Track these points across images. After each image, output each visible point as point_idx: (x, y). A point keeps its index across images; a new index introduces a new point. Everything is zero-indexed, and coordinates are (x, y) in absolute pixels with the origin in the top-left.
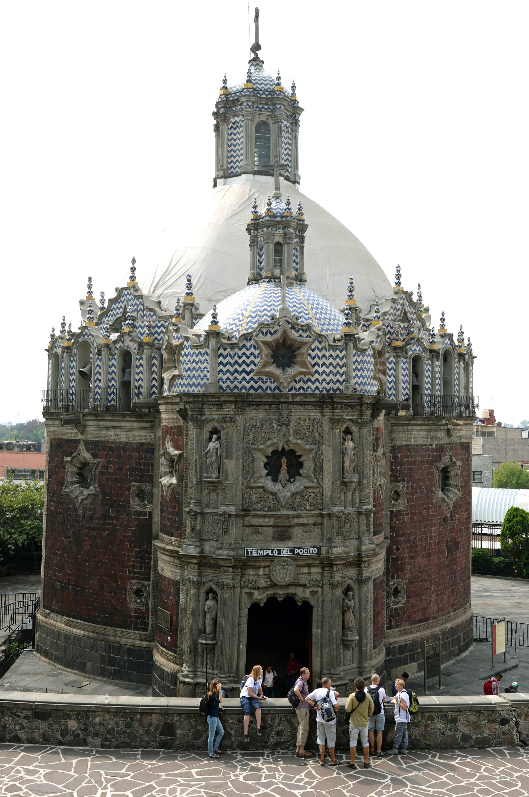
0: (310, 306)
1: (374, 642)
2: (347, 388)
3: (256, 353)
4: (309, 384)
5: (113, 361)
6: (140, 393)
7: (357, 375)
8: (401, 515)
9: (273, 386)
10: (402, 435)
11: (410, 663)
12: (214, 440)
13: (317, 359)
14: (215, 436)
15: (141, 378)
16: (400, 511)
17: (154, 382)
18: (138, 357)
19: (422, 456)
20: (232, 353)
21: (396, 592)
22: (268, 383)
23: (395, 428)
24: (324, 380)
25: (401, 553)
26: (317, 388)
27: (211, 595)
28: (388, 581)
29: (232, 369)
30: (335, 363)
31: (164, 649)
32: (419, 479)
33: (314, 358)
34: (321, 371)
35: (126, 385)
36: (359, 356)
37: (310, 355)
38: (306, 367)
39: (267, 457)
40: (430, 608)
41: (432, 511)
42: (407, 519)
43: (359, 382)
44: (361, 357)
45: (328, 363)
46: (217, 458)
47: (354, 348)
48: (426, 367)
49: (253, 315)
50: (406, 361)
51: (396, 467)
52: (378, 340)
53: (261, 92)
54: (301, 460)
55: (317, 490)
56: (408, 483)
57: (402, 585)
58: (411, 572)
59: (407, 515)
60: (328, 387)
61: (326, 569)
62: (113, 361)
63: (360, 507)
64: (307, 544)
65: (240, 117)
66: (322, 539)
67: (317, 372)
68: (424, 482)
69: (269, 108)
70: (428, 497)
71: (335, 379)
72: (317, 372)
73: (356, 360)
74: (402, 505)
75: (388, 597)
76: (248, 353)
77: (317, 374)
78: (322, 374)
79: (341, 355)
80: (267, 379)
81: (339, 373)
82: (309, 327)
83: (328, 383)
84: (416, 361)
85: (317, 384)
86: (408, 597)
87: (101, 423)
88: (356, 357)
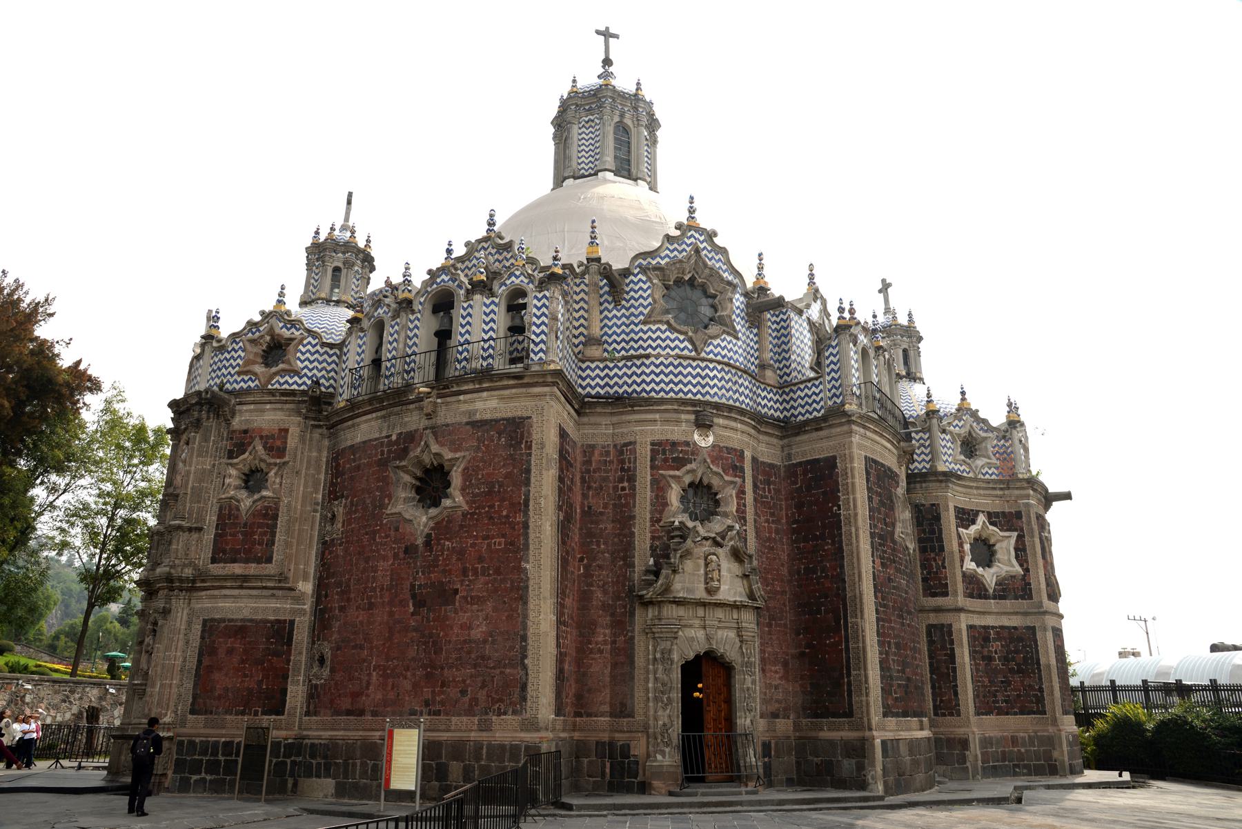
40: (368, 696)
42: (340, 551)
58: (339, 632)
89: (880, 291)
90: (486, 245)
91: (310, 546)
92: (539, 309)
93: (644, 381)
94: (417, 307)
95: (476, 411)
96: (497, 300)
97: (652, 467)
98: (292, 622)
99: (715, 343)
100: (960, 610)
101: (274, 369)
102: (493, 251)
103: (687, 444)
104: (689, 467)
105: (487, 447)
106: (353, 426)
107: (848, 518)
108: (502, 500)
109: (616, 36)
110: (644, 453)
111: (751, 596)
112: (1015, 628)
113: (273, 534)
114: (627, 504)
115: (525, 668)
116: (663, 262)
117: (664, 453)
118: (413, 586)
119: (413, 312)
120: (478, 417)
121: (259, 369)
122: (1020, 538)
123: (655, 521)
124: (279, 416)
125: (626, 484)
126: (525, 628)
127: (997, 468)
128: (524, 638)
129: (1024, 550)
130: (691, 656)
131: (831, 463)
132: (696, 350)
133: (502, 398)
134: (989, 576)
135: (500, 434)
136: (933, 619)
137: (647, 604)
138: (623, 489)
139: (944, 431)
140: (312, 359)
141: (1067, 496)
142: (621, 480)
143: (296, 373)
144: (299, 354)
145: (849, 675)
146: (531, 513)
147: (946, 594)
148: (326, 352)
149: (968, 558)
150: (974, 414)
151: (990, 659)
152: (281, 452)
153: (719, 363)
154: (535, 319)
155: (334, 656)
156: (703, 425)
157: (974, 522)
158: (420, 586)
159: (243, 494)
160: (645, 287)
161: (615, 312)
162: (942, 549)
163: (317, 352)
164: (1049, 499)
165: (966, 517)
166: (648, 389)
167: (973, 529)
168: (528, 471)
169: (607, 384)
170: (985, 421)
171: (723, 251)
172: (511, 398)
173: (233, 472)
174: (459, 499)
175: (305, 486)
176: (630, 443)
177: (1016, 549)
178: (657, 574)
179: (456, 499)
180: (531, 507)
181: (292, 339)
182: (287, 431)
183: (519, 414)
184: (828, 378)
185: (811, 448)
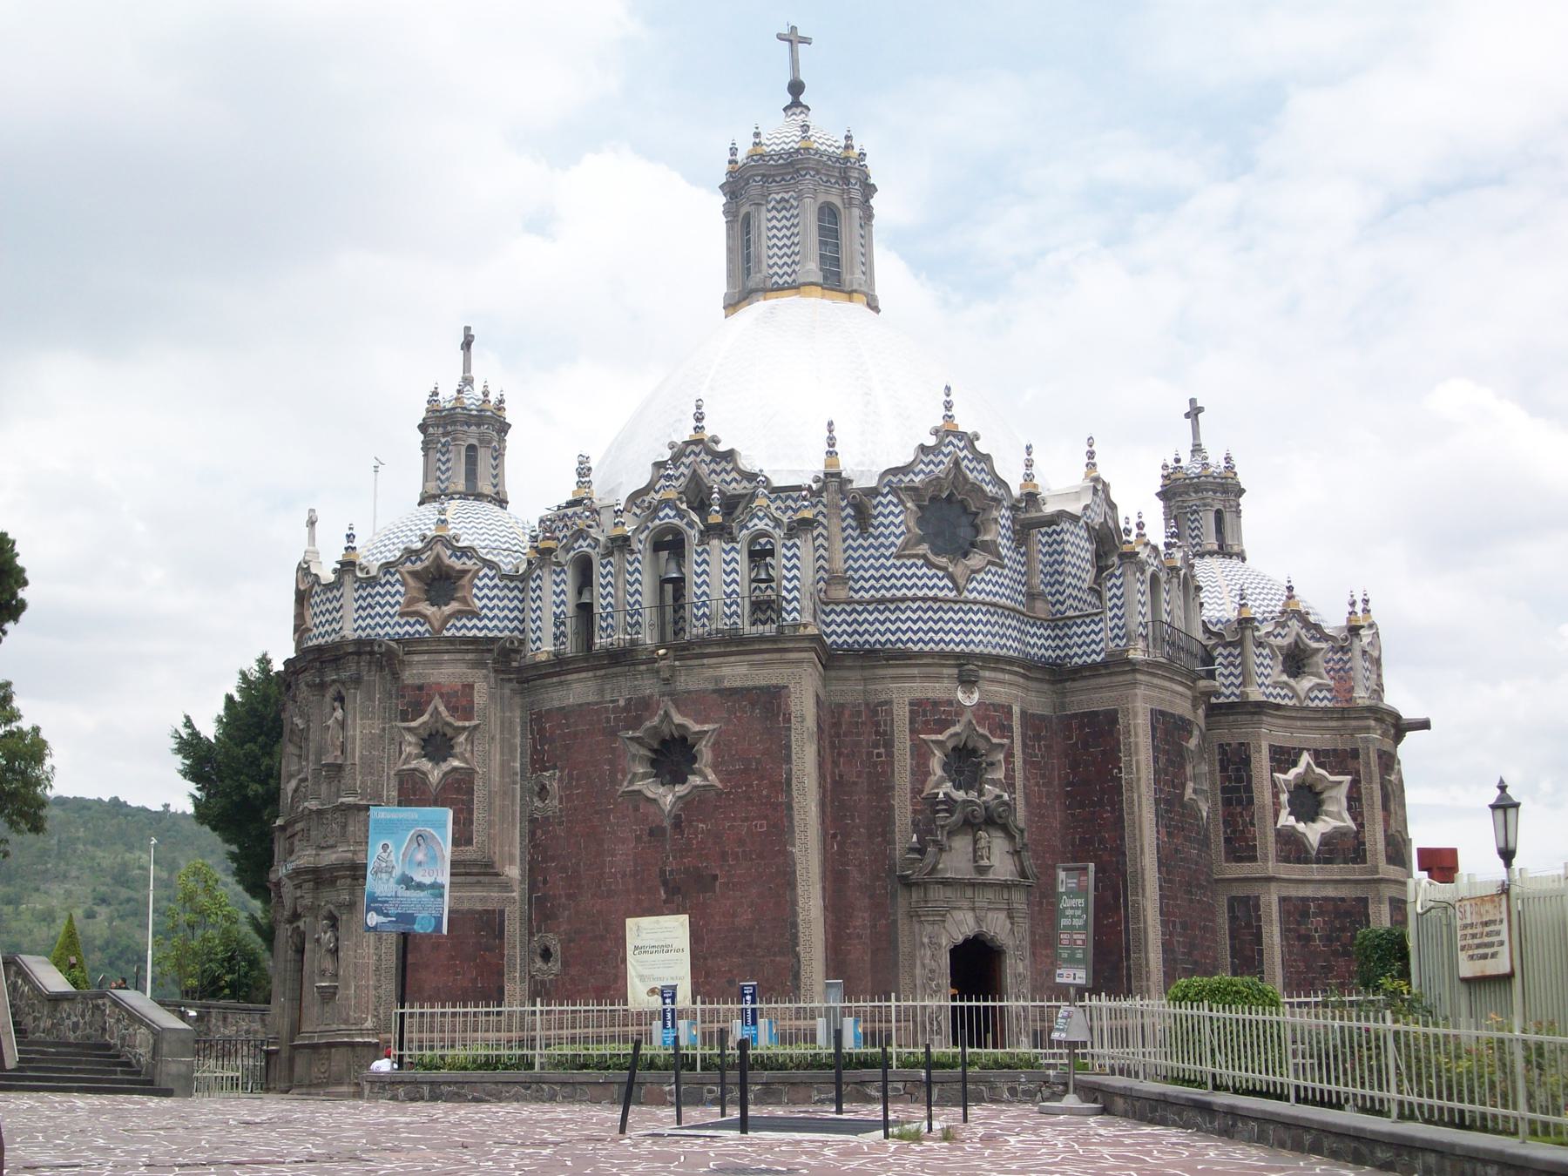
28: (531, 934)
86: (565, 964)
89: (1187, 415)
90: (697, 450)
91: (514, 825)
92: (789, 559)
93: (899, 629)
94: (636, 546)
95: (723, 677)
96: (738, 546)
97: (912, 731)
98: (502, 912)
99: (979, 577)
100: (1270, 879)
101: (447, 610)
102: (708, 459)
103: (950, 703)
104: (952, 730)
105: (739, 719)
106: (561, 683)
107: (1130, 783)
108: (761, 778)
109: (806, 41)
110: (902, 714)
111: (1023, 874)
112: (1342, 900)
113: (471, 812)
114: (884, 773)
115: (797, 956)
116: (917, 479)
117: (925, 715)
118: (663, 872)
119: (632, 552)
120: (726, 684)
121: (429, 610)
122: (1355, 783)
123: (916, 792)
124: (461, 669)
125: (882, 750)
126: (795, 914)
127: (1330, 690)
128: (795, 925)
129: (1359, 799)
130: (960, 939)
131: (1112, 717)
132: (956, 587)
133: (752, 664)
134: (1313, 832)
135: (753, 705)
136: (1240, 891)
137: (907, 884)
138: (879, 755)
139: (1260, 645)
140: (491, 595)
141: (1425, 725)
142: (877, 746)
143: (474, 614)
144: (475, 591)
145: (1128, 958)
146: (795, 794)
147: (1253, 859)
148: (506, 586)
149: (1284, 813)
150: (1302, 617)
151: (1308, 938)
152: (468, 713)
153: (984, 604)
154: (785, 572)
155: (564, 950)
156: (968, 682)
157: (1295, 764)
158: (671, 872)
159: (426, 765)
160: (897, 511)
161: (860, 541)
162: (1251, 801)
163: (496, 586)
164: (1399, 727)
165: (1284, 758)
166: (904, 638)
167: (1293, 773)
168: (788, 747)
169: (855, 631)
170: (1317, 627)
171: (987, 458)
172: (764, 664)
173: (409, 738)
174: (712, 777)
175: (502, 754)
176: (886, 703)
177: (1350, 799)
178: (921, 851)
179: (705, 776)
180: (794, 787)
181: (465, 572)
182: (471, 686)
183: (774, 682)
184: (1110, 614)
185: (1091, 698)
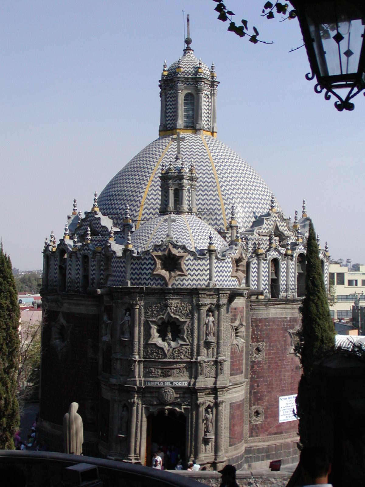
0: (192, 231)
1: (230, 442)
2: (209, 283)
3: (152, 262)
4: (184, 281)
5: (78, 262)
6: (93, 283)
7: (217, 275)
8: (261, 364)
9: (162, 283)
10: (262, 312)
11: (266, 460)
12: (127, 315)
13: (189, 266)
14: (128, 313)
15: (94, 273)
16: (260, 361)
17: (102, 276)
18: (93, 260)
19: (278, 325)
20: (138, 262)
21: (257, 413)
22: (159, 281)
23: (257, 307)
24: (194, 279)
25: (260, 389)
26: (189, 284)
27: (125, 408)
28: (250, 406)
29: (138, 272)
30: (201, 268)
31: (102, 441)
32: (275, 341)
33: (188, 265)
34: (192, 273)
35: (86, 277)
36: (219, 263)
37: (185, 264)
38: (183, 271)
39: (158, 326)
41: (286, 362)
42: (265, 366)
43: (219, 280)
44: (221, 263)
45: (197, 268)
46: (129, 326)
47: (216, 258)
48: (283, 265)
49: (155, 238)
50: (266, 263)
51: (257, 333)
52: (237, 252)
53: (188, 74)
54: (179, 328)
55: (189, 347)
56: (266, 343)
57: (261, 409)
58: (268, 401)
59: (265, 364)
60: (197, 283)
61: (194, 395)
62: (78, 262)
63: (217, 358)
64: (182, 379)
65: (174, 90)
66: (190, 377)
67: (189, 274)
68: (279, 342)
69: (193, 84)
70: (283, 353)
71: (201, 278)
72: (189, 274)
73: (217, 266)
74: (260, 357)
75: (250, 417)
76: (147, 262)
77: (189, 275)
78: (194, 275)
79: (206, 263)
80: (158, 279)
81: (205, 274)
82: (184, 248)
83: (197, 281)
84: (275, 262)
85: (189, 281)
86: (266, 418)
87: (71, 301)
88: (217, 264)
